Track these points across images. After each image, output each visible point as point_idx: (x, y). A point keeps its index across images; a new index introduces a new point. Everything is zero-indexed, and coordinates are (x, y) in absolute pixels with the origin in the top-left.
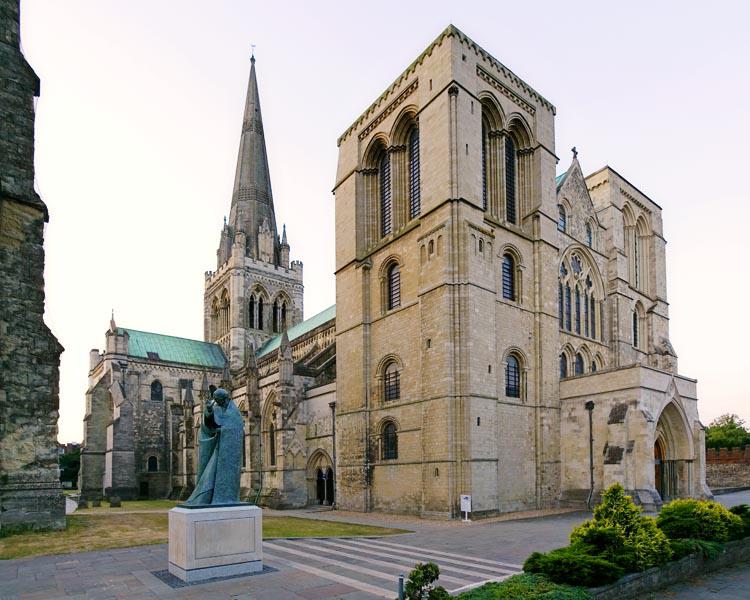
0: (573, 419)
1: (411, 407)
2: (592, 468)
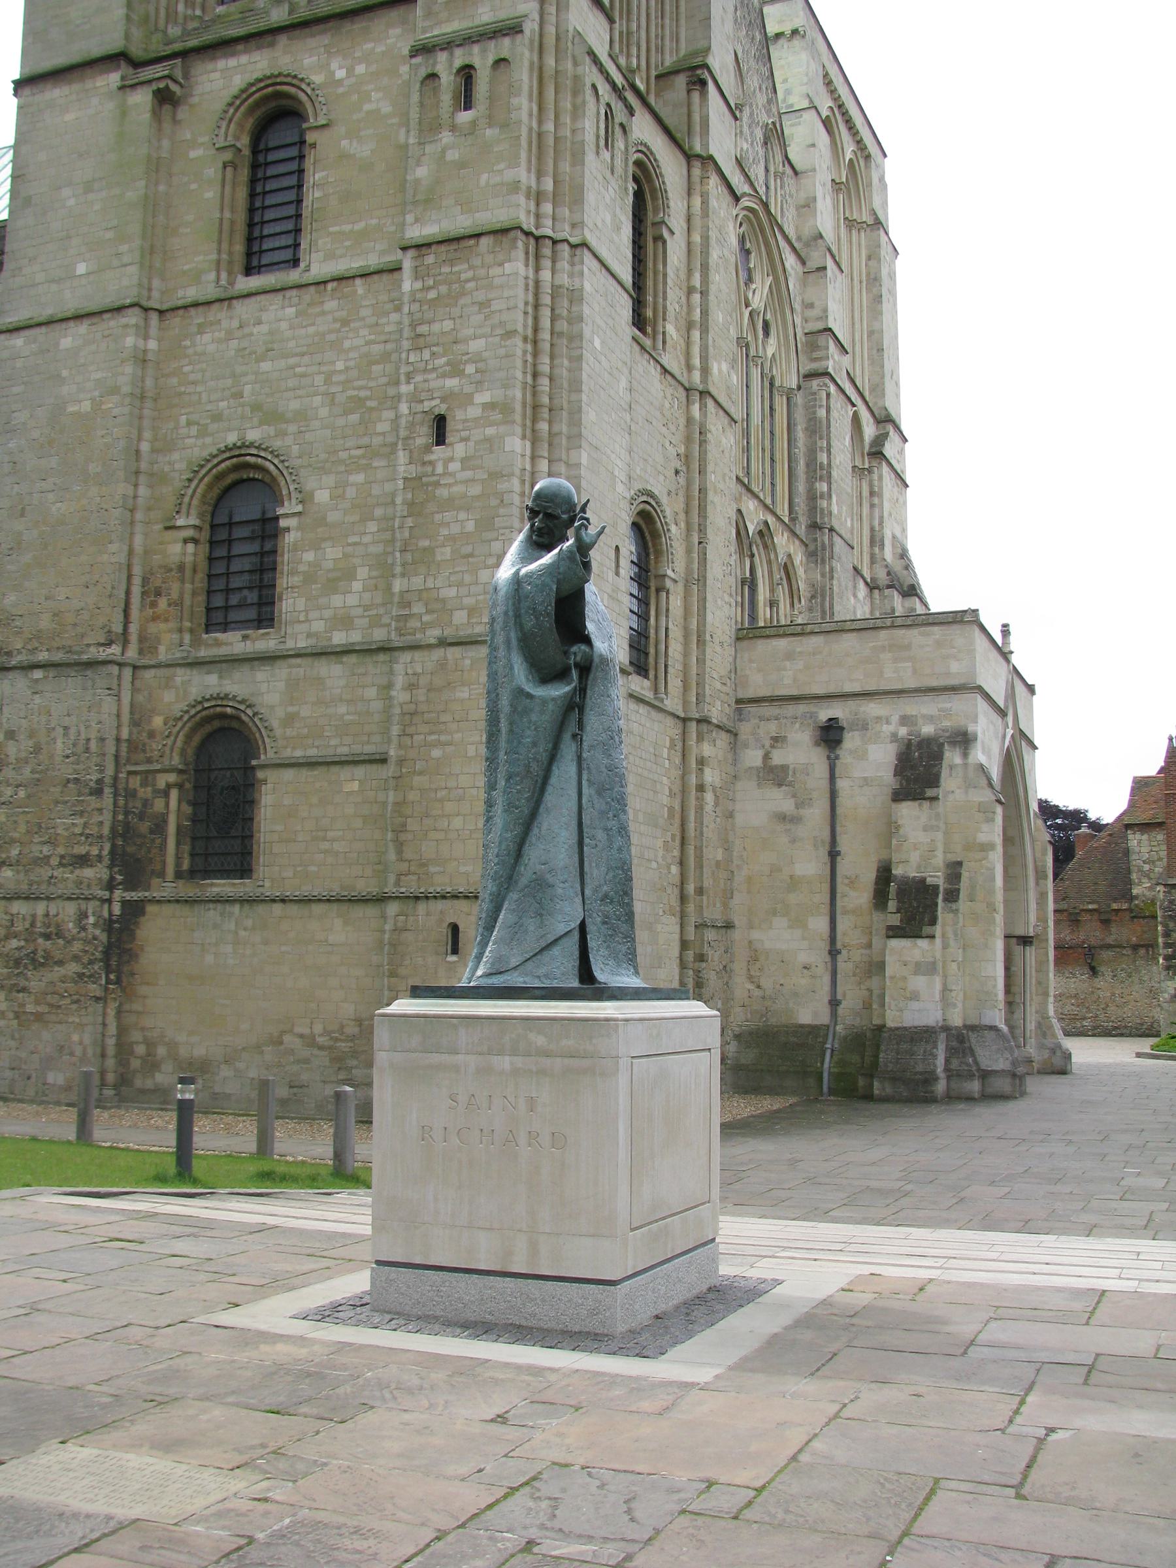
0: (775, 775)
1: (334, 673)
2: (834, 953)
